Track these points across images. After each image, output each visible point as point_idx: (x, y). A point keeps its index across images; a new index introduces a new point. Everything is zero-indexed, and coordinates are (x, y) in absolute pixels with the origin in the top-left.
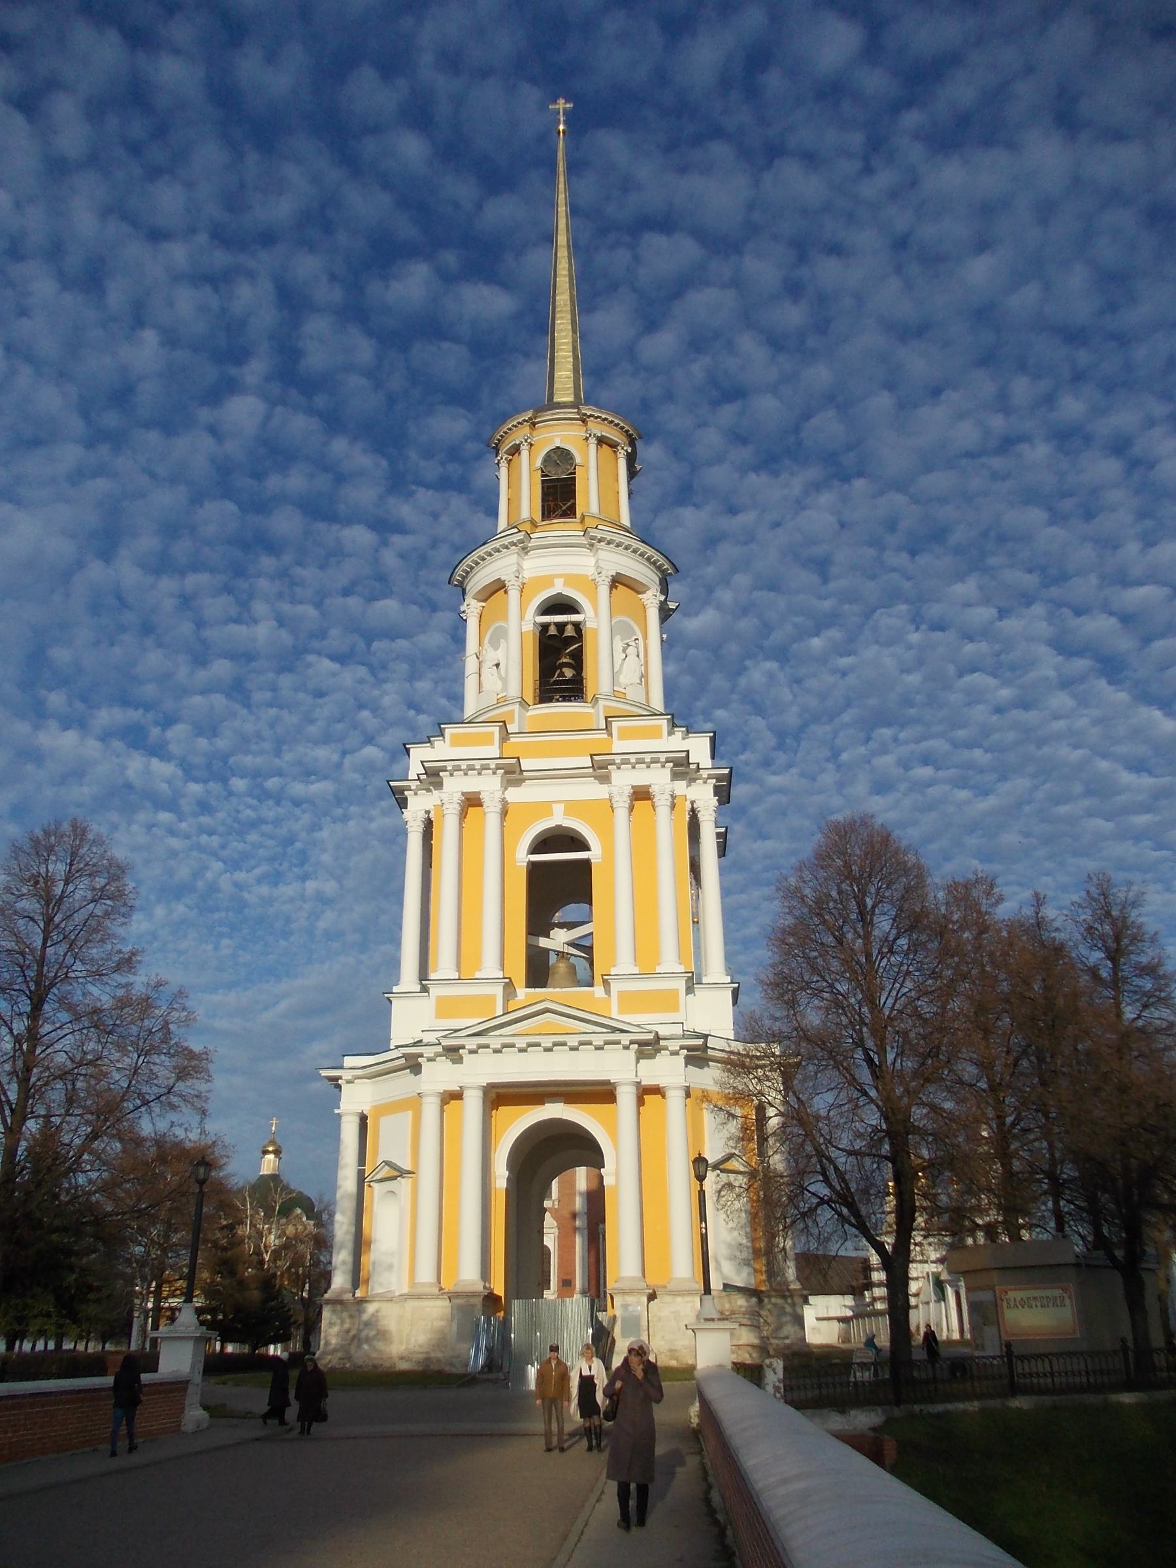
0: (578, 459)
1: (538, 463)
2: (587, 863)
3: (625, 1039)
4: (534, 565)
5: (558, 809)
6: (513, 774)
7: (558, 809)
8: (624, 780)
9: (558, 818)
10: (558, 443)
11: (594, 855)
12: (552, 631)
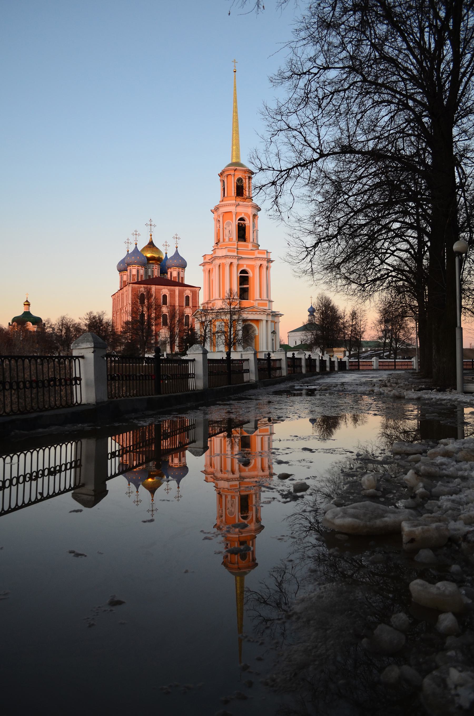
0: (244, 181)
1: (236, 181)
2: (248, 277)
3: (266, 313)
4: (240, 209)
5: (245, 266)
6: (240, 259)
7: (245, 266)
8: (259, 263)
9: (245, 268)
10: (240, 177)
11: (250, 274)
12: (240, 225)
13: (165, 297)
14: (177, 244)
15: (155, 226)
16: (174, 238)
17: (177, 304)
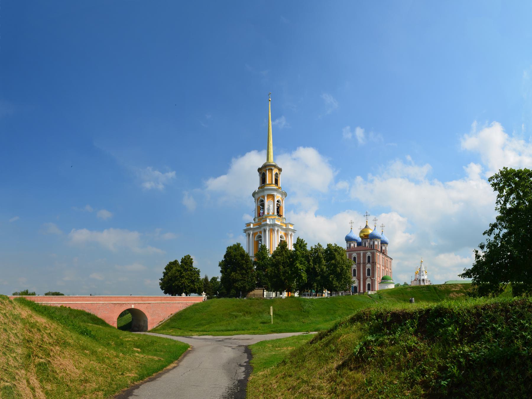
13: (355, 258)
17: (362, 262)
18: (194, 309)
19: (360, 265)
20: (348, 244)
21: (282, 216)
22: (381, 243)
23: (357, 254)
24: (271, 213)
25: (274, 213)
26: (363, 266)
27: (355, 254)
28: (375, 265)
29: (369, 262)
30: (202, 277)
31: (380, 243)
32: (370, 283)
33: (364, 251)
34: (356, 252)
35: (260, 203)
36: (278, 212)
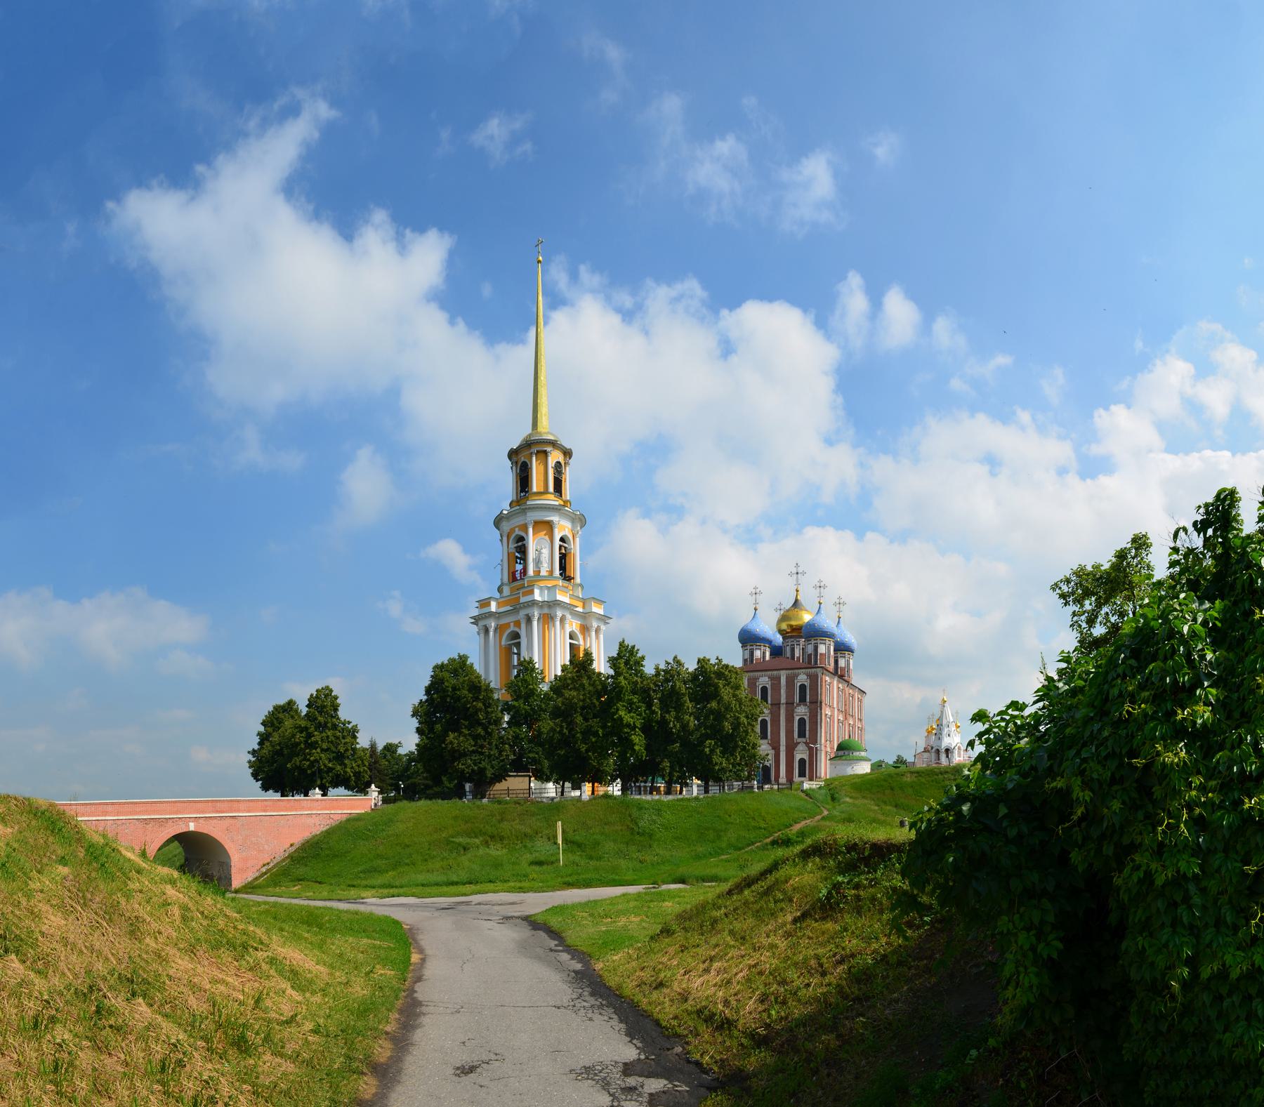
13: (764, 690)
14: (820, 596)
15: (804, 573)
16: (815, 587)
17: (783, 700)
18: (349, 829)
19: (779, 708)
20: (747, 652)
21: (573, 578)
22: (835, 650)
23: (771, 678)
24: (544, 573)
25: (551, 572)
26: (787, 710)
27: (766, 679)
28: (819, 711)
29: (803, 699)
30: (363, 741)
31: (832, 648)
32: (806, 757)
33: (790, 672)
34: (769, 673)
35: (516, 545)
36: (563, 568)
